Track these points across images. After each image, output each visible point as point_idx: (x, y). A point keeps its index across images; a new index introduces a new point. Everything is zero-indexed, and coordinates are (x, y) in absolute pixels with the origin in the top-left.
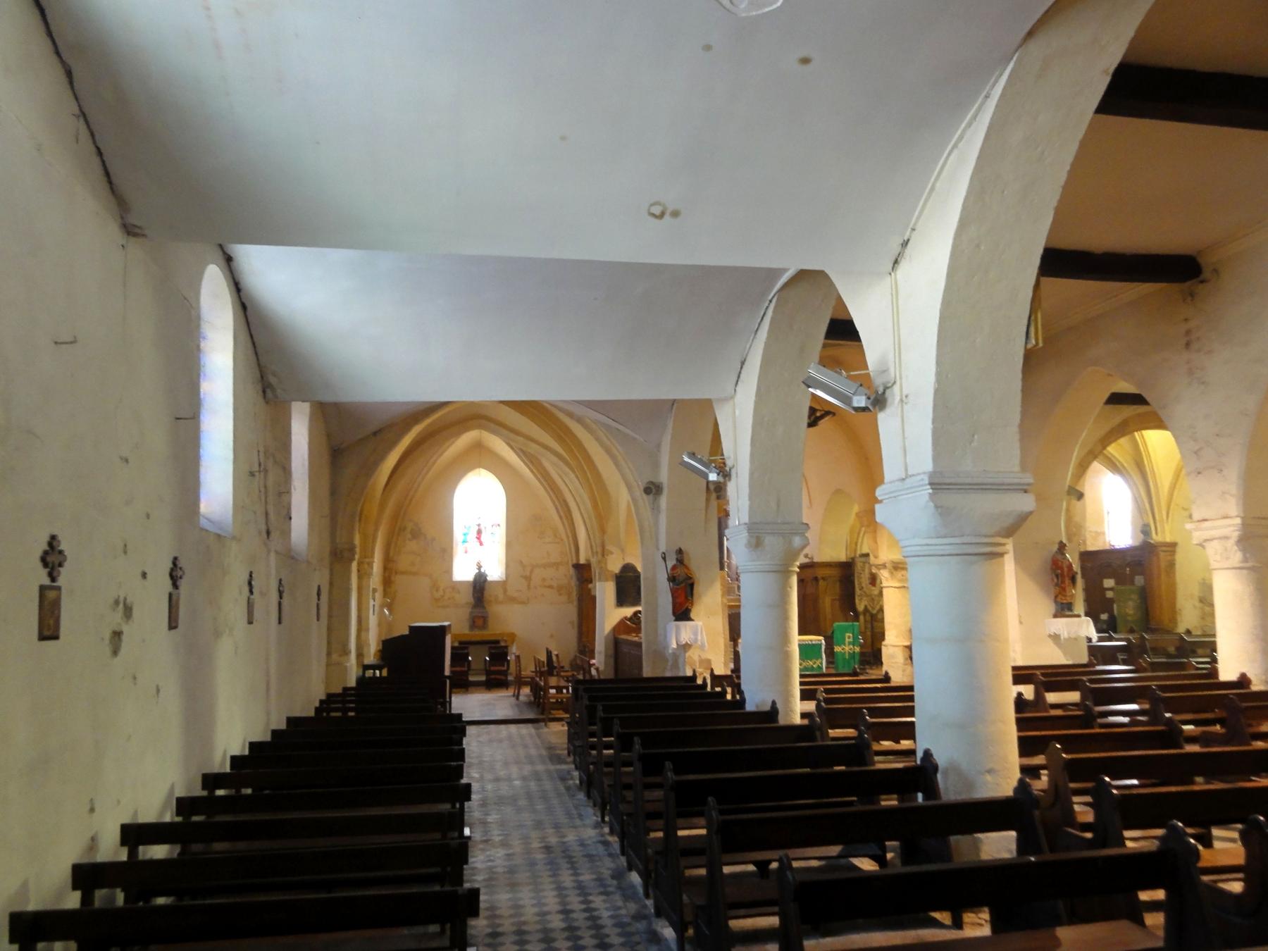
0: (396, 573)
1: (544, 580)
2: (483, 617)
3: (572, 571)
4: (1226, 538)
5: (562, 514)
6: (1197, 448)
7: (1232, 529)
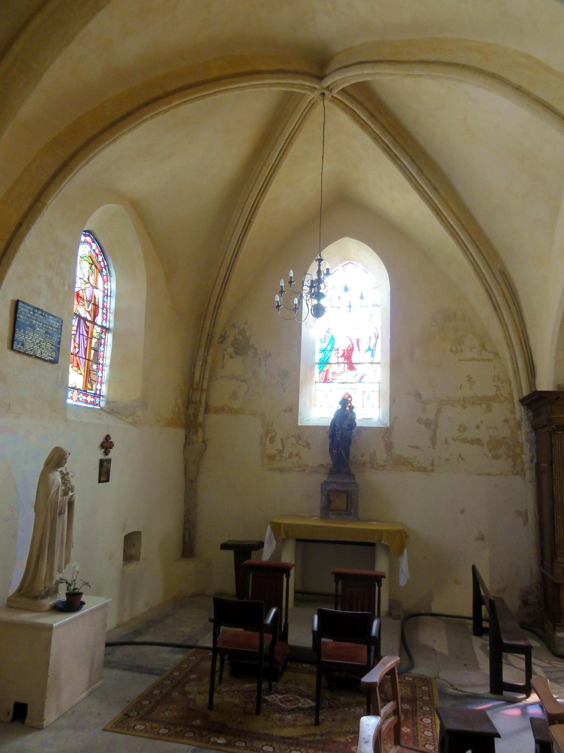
0: (207, 410)
1: (462, 428)
2: (346, 492)
3: (520, 411)
5: (500, 300)
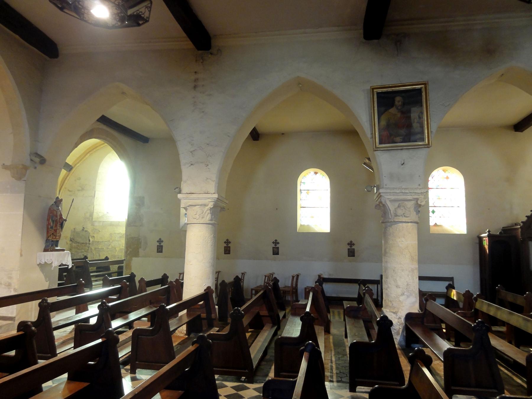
4: (205, 205)
6: (192, 150)
7: (210, 200)
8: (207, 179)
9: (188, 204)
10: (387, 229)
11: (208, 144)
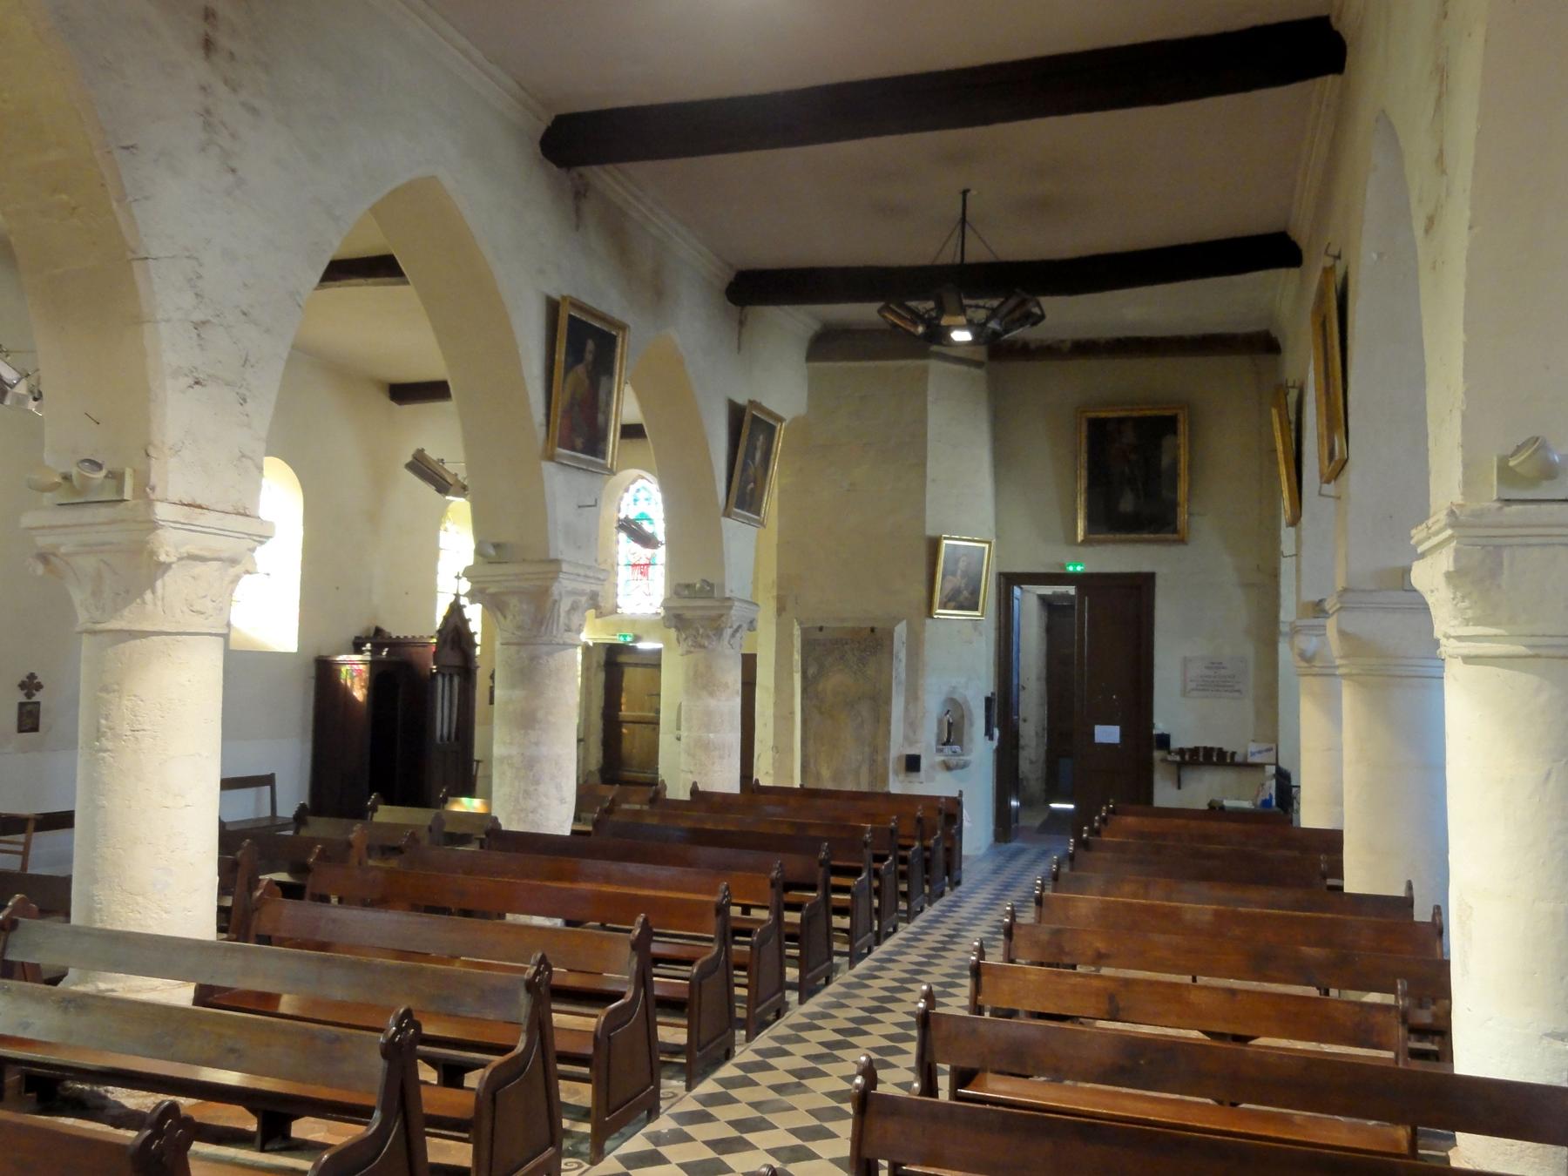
6: (198, 316)
8: (243, 456)
9: (184, 550)
10: (541, 661)
11: (245, 314)
